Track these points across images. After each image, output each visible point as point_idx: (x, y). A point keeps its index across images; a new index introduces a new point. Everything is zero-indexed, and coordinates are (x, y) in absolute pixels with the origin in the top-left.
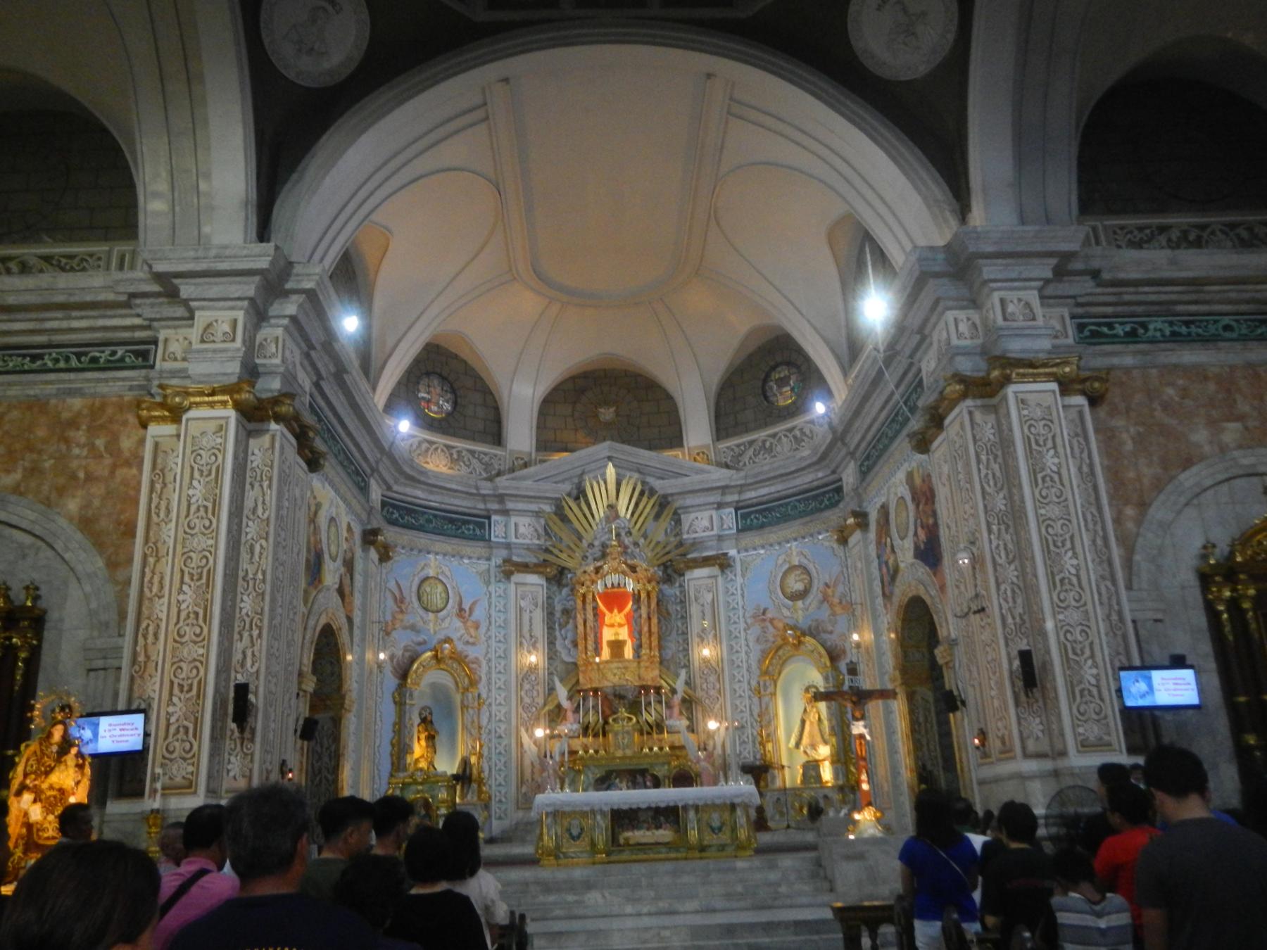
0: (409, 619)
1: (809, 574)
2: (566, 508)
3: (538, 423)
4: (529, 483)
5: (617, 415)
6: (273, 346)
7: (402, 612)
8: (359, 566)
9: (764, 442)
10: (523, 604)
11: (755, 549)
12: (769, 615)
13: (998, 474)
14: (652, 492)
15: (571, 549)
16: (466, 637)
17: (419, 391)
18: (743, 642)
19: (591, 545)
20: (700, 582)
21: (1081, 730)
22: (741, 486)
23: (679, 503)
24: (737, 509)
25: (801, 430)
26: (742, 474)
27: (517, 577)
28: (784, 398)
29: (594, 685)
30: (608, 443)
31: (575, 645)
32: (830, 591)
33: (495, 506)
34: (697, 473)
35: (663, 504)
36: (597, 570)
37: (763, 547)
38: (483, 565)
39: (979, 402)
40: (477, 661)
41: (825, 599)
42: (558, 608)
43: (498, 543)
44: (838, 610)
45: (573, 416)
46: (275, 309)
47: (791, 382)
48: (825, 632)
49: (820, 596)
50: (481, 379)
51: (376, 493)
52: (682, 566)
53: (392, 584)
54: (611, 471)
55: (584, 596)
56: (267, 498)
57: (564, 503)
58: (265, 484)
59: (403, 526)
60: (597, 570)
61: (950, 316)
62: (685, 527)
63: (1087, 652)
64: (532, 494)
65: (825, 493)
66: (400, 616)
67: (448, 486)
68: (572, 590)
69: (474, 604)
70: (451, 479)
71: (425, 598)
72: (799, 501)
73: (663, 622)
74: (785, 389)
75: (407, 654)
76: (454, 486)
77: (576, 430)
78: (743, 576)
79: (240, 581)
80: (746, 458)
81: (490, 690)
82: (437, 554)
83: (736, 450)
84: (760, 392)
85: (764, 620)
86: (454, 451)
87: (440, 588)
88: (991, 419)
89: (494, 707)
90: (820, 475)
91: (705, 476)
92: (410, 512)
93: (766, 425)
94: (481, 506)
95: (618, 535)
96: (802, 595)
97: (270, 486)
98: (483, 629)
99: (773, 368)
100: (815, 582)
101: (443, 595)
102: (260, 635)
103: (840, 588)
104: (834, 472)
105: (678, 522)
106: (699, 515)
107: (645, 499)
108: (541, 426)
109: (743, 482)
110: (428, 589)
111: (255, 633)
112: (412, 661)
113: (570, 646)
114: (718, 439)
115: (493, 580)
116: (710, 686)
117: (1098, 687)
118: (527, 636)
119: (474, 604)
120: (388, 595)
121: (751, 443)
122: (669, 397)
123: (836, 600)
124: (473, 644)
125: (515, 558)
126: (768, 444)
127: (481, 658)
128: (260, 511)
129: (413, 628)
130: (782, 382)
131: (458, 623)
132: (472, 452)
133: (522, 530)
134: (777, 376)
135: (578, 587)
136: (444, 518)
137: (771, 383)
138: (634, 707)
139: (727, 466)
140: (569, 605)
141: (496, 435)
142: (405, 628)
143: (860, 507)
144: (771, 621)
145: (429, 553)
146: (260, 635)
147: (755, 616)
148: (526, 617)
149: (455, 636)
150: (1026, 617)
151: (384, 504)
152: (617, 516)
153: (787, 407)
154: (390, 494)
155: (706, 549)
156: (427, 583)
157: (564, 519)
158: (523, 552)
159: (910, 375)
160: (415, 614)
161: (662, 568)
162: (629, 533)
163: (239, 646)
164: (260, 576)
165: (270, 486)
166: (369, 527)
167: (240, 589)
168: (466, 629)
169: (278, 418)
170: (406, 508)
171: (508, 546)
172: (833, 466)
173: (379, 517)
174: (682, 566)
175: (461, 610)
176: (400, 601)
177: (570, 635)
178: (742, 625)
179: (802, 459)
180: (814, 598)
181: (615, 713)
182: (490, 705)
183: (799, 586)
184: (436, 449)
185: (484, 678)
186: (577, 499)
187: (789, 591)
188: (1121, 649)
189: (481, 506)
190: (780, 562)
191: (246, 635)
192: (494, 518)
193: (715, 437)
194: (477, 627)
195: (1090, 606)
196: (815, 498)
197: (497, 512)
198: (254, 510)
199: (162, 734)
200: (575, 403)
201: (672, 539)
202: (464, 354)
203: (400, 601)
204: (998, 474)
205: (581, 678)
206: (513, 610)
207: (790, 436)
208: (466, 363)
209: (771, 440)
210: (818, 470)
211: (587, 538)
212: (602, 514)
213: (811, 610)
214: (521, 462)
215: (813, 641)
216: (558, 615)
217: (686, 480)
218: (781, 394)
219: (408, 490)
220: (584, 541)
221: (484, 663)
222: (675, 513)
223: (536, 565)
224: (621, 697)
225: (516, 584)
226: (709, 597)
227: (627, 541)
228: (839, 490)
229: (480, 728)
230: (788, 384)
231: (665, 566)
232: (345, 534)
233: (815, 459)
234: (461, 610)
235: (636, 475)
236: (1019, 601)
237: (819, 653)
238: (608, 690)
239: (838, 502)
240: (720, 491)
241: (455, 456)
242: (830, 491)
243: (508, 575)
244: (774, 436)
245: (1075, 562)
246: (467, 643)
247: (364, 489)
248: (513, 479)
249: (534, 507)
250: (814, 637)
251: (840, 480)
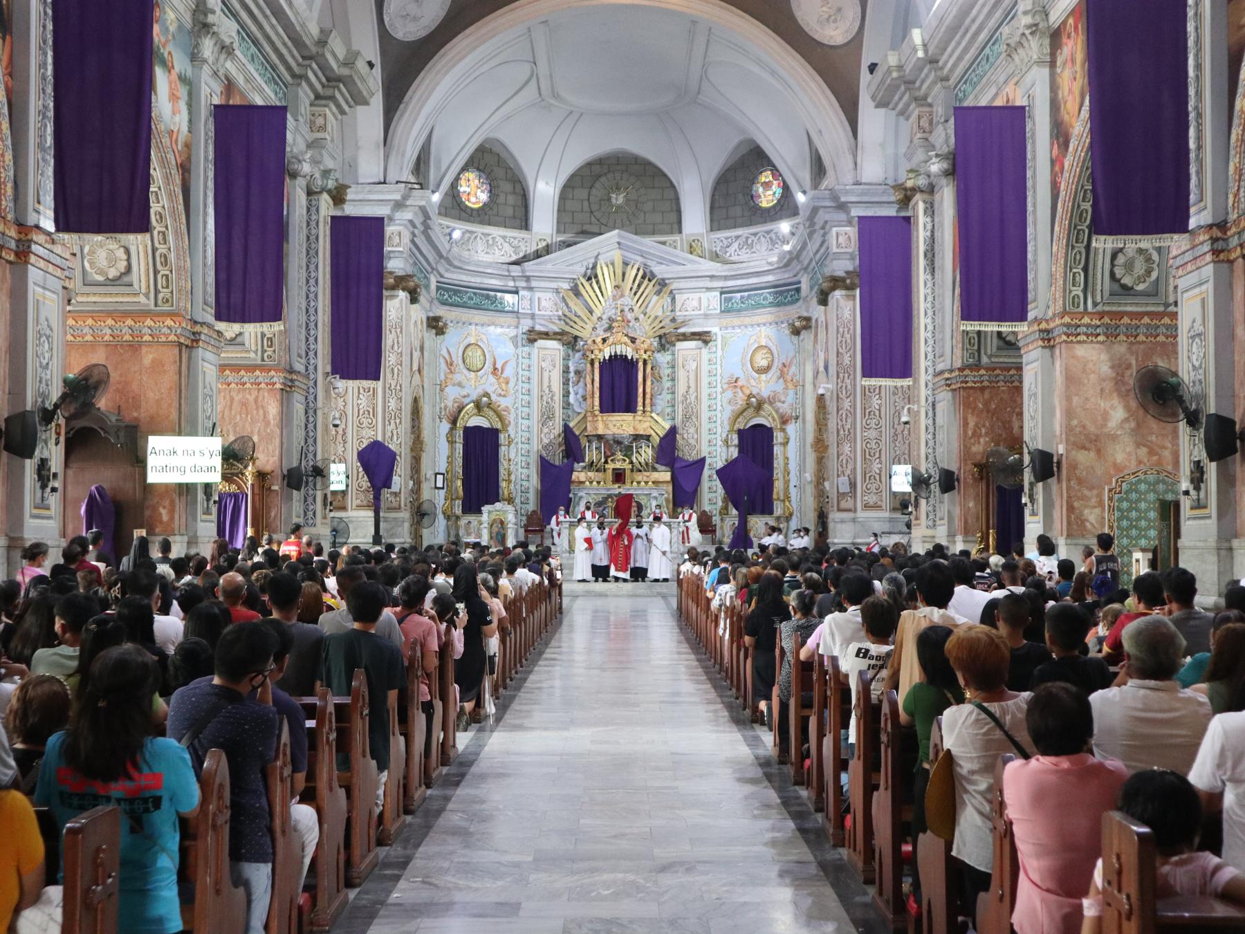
0: (457, 377)
1: (772, 355)
2: (580, 286)
3: (559, 206)
4: (549, 266)
5: (627, 200)
6: (397, 238)
7: (451, 372)
8: (426, 345)
9: (747, 238)
10: (544, 365)
11: (733, 328)
12: (740, 383)
13: (849, 341)
14: (653, 276)
15: (582, 320)
16: (500, 391)
18: (719, 404)
19: (600, 319)
20: (685, 353)
21: (866, 498)
23: (674, 286)
24: (722, 293)
25: (776, 233)
26: (727, 267)
27: (541, 343)
28: (768, 197)
29: (600, 432)
30: (616, 231)
31: (584, 398)
32: (785, 370)
33: (523, 284)
35: (663, 284)
36: (604, 340)
37: (739, 327)
38: (512, 332)
39: (844, 292)
40: (507, 409)
41: (782, 375)
42: (572, 369)
43: (524, 314)
44: (790, 385)
46: (398, 215)
47: (774, 187)
48: (780, 401)
49: (779, 372)
51: (433, 286)
52: (673, 339)
53: (444, 352)
54: (617, 256)
55: (592, 360)
56: (400, 339)
58: (399, 330)
59: (451, 305)
60: (604, 340)
61: (834, 230)
62: (677, 309)
63: (877, 455)
65: (789, 290)
66: (450, 376)
68: (584, 355)
69: (506, 362)
70: (490, 265)
71: (468, 361)
72: (770, 293)
73: (656, 383)
75: (456, 405)
76: (489, 271)
78: (722, 350)
79: (387, 390)
80: (731, 250)
81: (517, 432)
82: (476, 325)
83: (725, 241)
85: (736, 387)
86: (490, 238)
87: (479, 352)
88: (851, 303)
89: (520, 446)
90: (786, 276)
91: (695, 267)
92: (456, 292)
93: (750, 223)
94: (511, 284)
95: (622, 311)
96: (766, 370)
97: (401, 332)
98: (511, 384)
100: (776, 361)
101: (482, 358)
102: (400, 423)
103: (793, 369)
104: (795, 276)
105: (673, 299)
106: (691, 296)
107: (646, 282)
110: (470, 354)
111: (398, 421)
112: (460, 412)
113: (581, 399)
114: (711, 230)
115: (520, 344)
116: (690, 436)
117: (880, 475)
118: (547, 391)
119: (506, 362)
120: (442, 360)
121: (737, 237)
123: (789, 378)
124: (504, 396)
125: (538, 328)
126: (750, 241)
127: (510, 407)
128: (396, 347)
129: (460, 385)
130: (767, 185)
131: (492, 379)
132: (504, 238)
133: (543, 303)
135: (588, 353)
136: (482, 295)
137: (759, 185)
138: (628, 451)
139: (715, 257)
140: (581, 367)
141: (523, 221)
142: (454, 385)
143: (807, 311)
144: (741, 388)
145: (470, 324)
146: (400, 423)
147: (729, 383)
148: (546, 375)
149: (489, 392)
150: (852, 431)
151: (438, 288)
152: (622, 296)
153: (768, 210)
154: (442, 280)
155: (694, 325)
156: (470, 349)
157: (577, 293)
158: (543, 322)
159: (822, 250)
160: (462, 375)
161: (657, 339)
162: (632, 310)
163: (389, 428)
164: (398, 387)
165: (401, 332)
166: (431, 315)
167: (387, 395)
168: (499, 384)
169: (403, 290)
170: (454, 290)
171: (533, 316)
172: (795, 272)
173: (436, 302)
174: (673, 339)
175: (495, 369)
176: (450, 364)
177: (581, 392)
178: (719, 389)
179: (770, 264)
180: (774, 372)
181: (613, 454)
182: (517, 443)
183: (764, 363)
184: (476, 237)
185: (512, 423)
186: (589, 279)
187: (756, 365)
188: (906, 452)
189: (511, 284)
190: (752, 341)
191: (392, 422)
192: (521, 293)
193: (709, 228)
194: (507, 383)
195: (883, 429)
196: (781, 293)
197: (524, 288)
198: (393, 348)
199: (355, 478)
201: (669, 313)
202: (496, 149)
203: (450, 364)
204: (849, 341)
205: (589, 428)
206: (535, 369)
207: (768, 237)
209: (753, 238)
211: (598, 313)
212: (610, 293)
213: (771, 383)
214: (544, 244)
215: (770, 408)
216: (572, 375)
217: (681, 268)
219: (455, 276)
221: (512, 411)
222: (671, 292)
223: (556, 333)
224: (618, 443)
225: (539, 348)
226: (694, 366)
227: (630, 316)
228: (798, 290)
229: (510, 460)
231: (660, 337)
232: (420, 327)
233: (781, 265)
234: (495, 369)
235: (639, 259)
236: (849, 420)
237: (773, 417)
238: (610, 438)
239: (798, 300)
241: (491, 242)
242: (791, 290)
243: (532, 341)
244: (755, 234)
245: (879, 402)
246: (500, 395)
247: (427, 287)
248: (537, 264)
249: (554, 285)
250: (771, 403)
251: (799, 282)
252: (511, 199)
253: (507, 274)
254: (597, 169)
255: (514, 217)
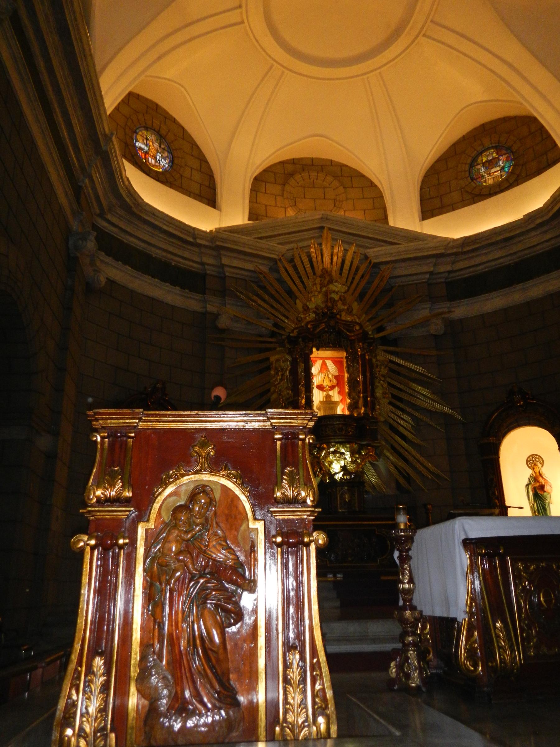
17: (137, 140)
22: (456, 254)
34: (412, 242)
45: (283, 196)
47: (501, 163)
50: (198, 147)
57: (279, 264)
64: (250, 251)
67: (165, 227)
74: (493, 170)
76: (171, 230)
77: (285, 208)
84: (467, 174)
99: (481, 153)
108: (253, 200)
109: (460, 250)
122: (372, 185)
134: (484, 160)
137: (479, 167)
193: (421, 218)
200: (284, 185)
208: (183, 128)
210: (545, 232)
217: (401, 248)
218: (489, 174)
220: (298, 301)
230: (497, 165)
240: (434, 260)
252: (197, 176)
253: (191, 240)
254: (290, 168)
255: (200, 196)
